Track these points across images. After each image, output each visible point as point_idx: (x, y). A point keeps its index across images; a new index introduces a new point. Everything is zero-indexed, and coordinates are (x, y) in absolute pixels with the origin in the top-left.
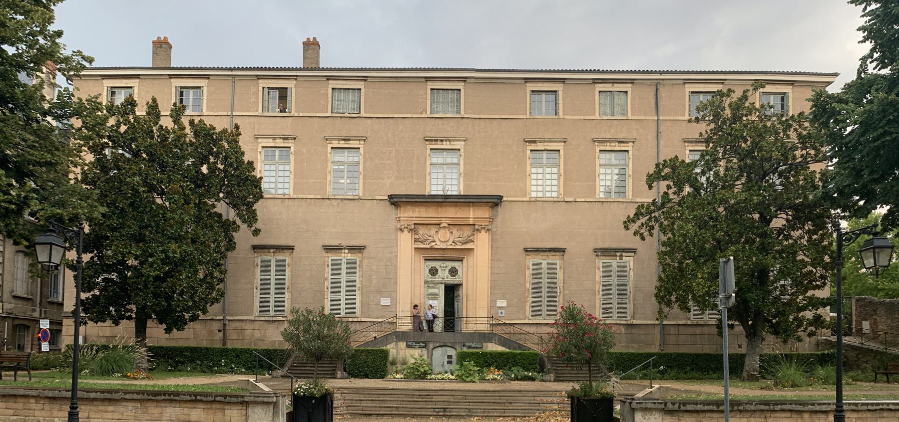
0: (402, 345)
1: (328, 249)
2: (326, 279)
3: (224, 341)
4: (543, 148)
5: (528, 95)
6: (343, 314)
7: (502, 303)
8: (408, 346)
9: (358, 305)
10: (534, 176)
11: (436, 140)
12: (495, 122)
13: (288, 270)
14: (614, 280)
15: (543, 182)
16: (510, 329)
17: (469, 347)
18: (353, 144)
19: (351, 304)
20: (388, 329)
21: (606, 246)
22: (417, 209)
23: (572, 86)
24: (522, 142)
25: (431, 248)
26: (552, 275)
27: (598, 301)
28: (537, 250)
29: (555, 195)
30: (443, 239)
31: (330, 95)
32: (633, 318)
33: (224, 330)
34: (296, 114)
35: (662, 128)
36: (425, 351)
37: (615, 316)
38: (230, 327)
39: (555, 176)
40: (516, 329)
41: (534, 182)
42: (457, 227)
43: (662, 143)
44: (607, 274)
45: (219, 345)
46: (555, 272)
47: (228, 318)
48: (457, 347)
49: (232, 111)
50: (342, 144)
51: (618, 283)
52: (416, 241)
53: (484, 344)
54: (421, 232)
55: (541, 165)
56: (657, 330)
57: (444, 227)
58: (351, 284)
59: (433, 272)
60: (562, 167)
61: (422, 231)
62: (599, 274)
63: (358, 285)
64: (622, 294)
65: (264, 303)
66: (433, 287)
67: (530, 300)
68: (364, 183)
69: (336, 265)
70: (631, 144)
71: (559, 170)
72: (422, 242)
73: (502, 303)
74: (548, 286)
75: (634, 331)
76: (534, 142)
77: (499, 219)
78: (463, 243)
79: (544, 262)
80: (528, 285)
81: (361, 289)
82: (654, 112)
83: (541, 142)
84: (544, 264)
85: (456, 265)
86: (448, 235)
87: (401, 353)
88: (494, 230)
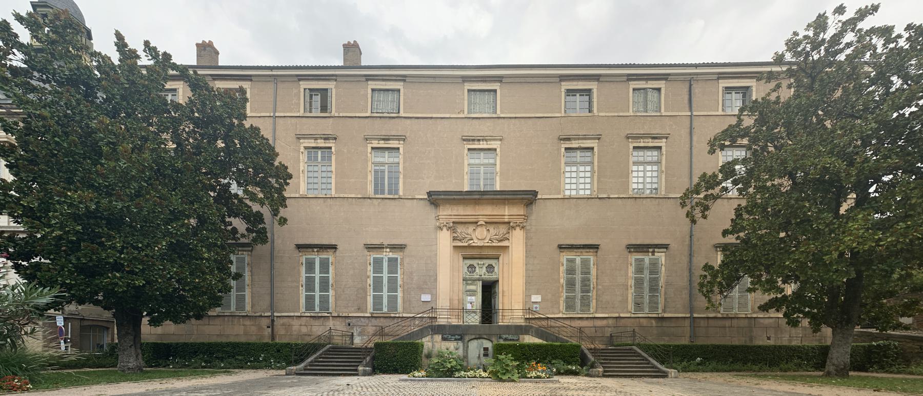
1: (370, 248)
2: (368, 277)
3: (273, 336)
4: (576, 146)
5: (563, 94)
6: (385, 310)
7: (536, 298)
8: (444, 339)
9: (400, 301)
10: (568, 175)
11: (473, 140)
12: (530, 122)
13: (331, 269)
14: (646, 275)
15: (577, 180)
16: (544, 323)
17: (506, 339)
18: (393, 144)
19: (393, 300)
20: (427, 323)
21: (638, 243)
23: (607, 84)
25: (469, 247)
26: (586, 271)
27: (630, 296)
28: (572, 247)
29: (588, 192)
30: (480, 236)
31: (369, 96)
32: (664, 311)
33: (272, 325)
34: (337, 115)
35: (695, 124)
36: (460, 344)
37: (647, 310)
38: (278, 322)
39: (588, 174)
40: (552, 323)
41: (568, 181)
43: (695, 138)
44: (639, 270)
45: (267, 340)
46: (589, 269)
47: (276, 314)
49: (275, 112)
50: (382, 144)
51: (650, 278)
52: (455, 239)
53: (521, 336)
55: (574, 164)
56: (687, 323)
57: (481, 225)
58: (393, 283)
60: (596, 163)
61: (460, 229)
62: (631, 270)
63: (400, 282)
64: (654, 288)
65: (310, 300)
66: (471, 284)
67: (564, 295)
68: (404, 183)
69: (378, 263)
70: (664, 140)
71: (593, 168)
72: (460, 240)
73: (536, 298)
75: (664, 324)
76: (569, 139)
77: (533, 217)
80: (562, 281)
81: (402, 286)
82: (687, 109)
83: (575, 139)
84: (578, 260)
86: (485, 232)
87: (437, 346)
88: (528, 228)
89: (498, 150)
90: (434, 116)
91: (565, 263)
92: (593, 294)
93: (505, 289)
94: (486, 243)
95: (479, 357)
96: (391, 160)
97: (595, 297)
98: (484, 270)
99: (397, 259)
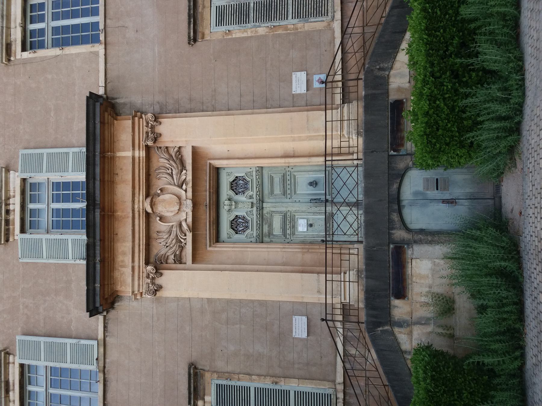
0: (400, 308)
7: (299, 83)
22: (120, 258)
24: (11, 69)
25: (194, 228)
28: (194, 17)
30: (174, 207)
42: (154, 181)
48: (401, 165)
54: (163, 251)
57: (152, 205)
61: (160, 248)
63: (267, 384)
66: (270, 226)
67: (291, 22)
72: (182, 248)
73: (299, 83)
76: (9, 46)
78: (183, 166)
81: (276, 378)
85: (225, 181)
86: (166, 197)
88: (157, 108)
89: (25, 176)
91: (223, 28)
94: (187, 194)
95: (451, 202)
96: (42, 379)
98: (241, 198)
99: (218, 386)
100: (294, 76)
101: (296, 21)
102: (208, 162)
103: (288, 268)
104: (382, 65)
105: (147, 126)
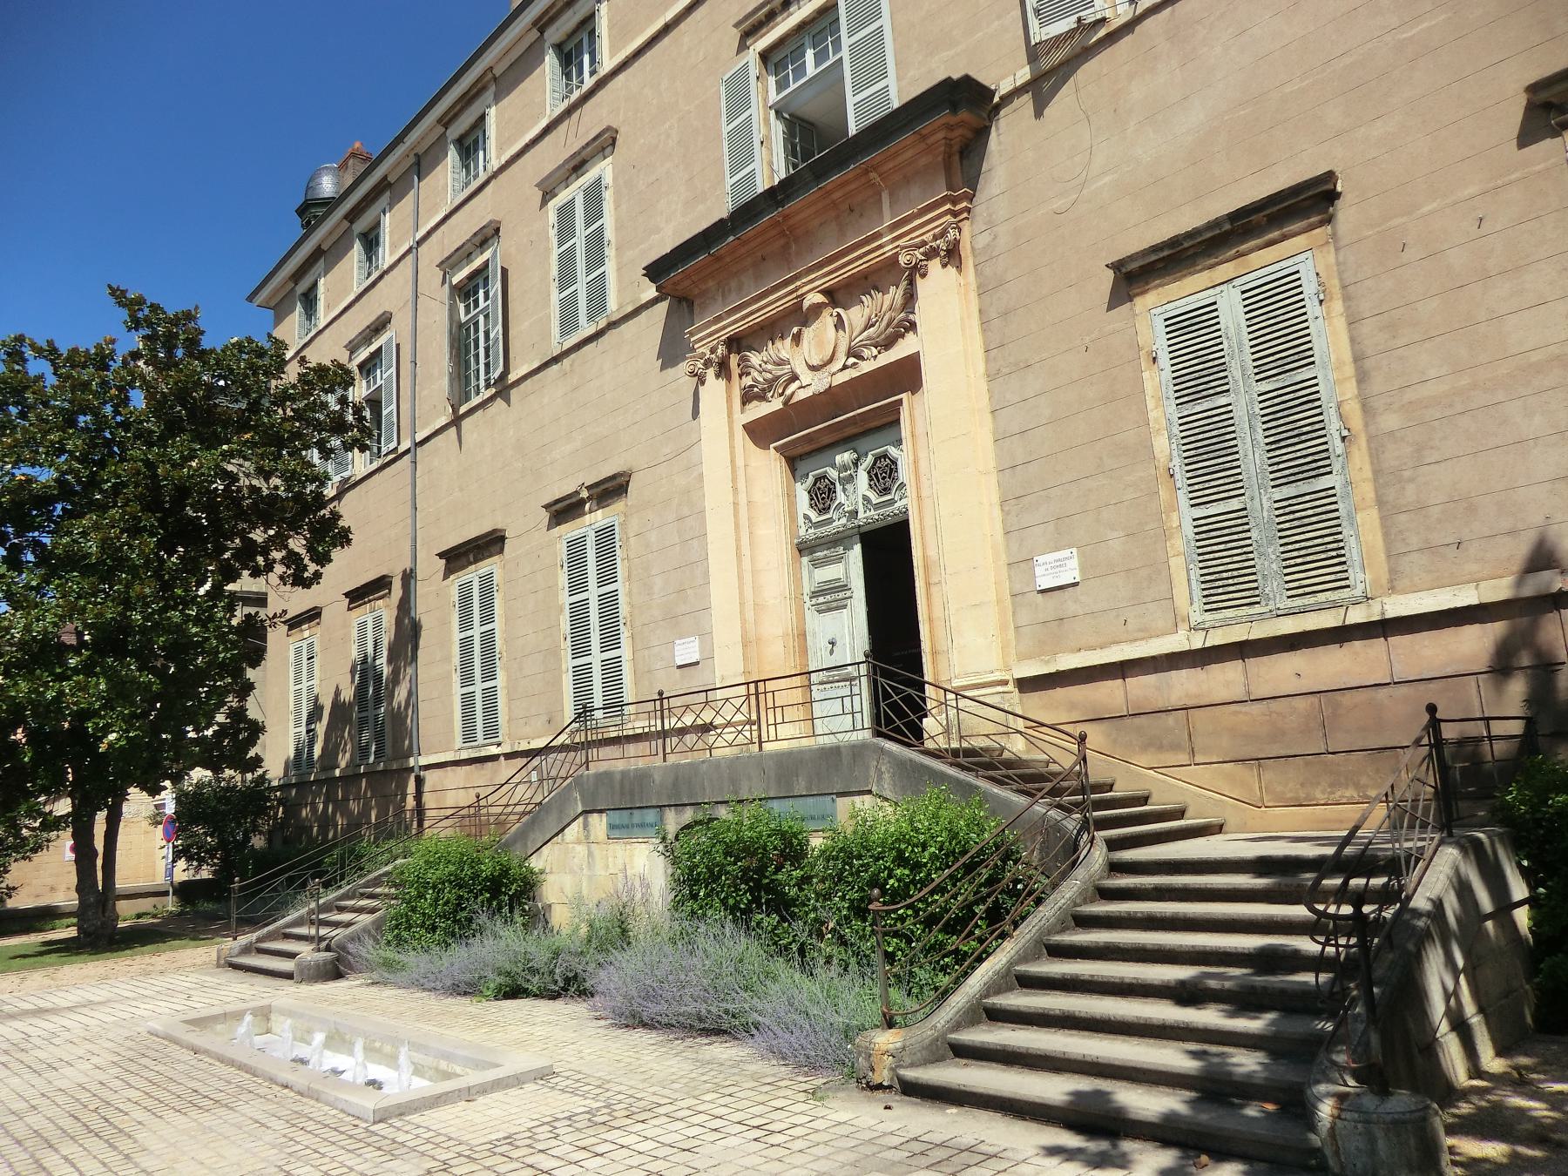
30: (816, 359)
47: (423, 761)
59: (822, 496)
66: (826, 562)
67: (1184, 517)
73: (1058, 567)
74: (1270, 418)
79: (1223, 293)
90: (670, 15)
92: (1351, 476)
93: (932, 553)
97: (1366, 490)
100: (1066, 553)
101: (1189, 530)
102: (904, 396)
103: (750, 615)
104: (886, 776)
105: (935, 238)
